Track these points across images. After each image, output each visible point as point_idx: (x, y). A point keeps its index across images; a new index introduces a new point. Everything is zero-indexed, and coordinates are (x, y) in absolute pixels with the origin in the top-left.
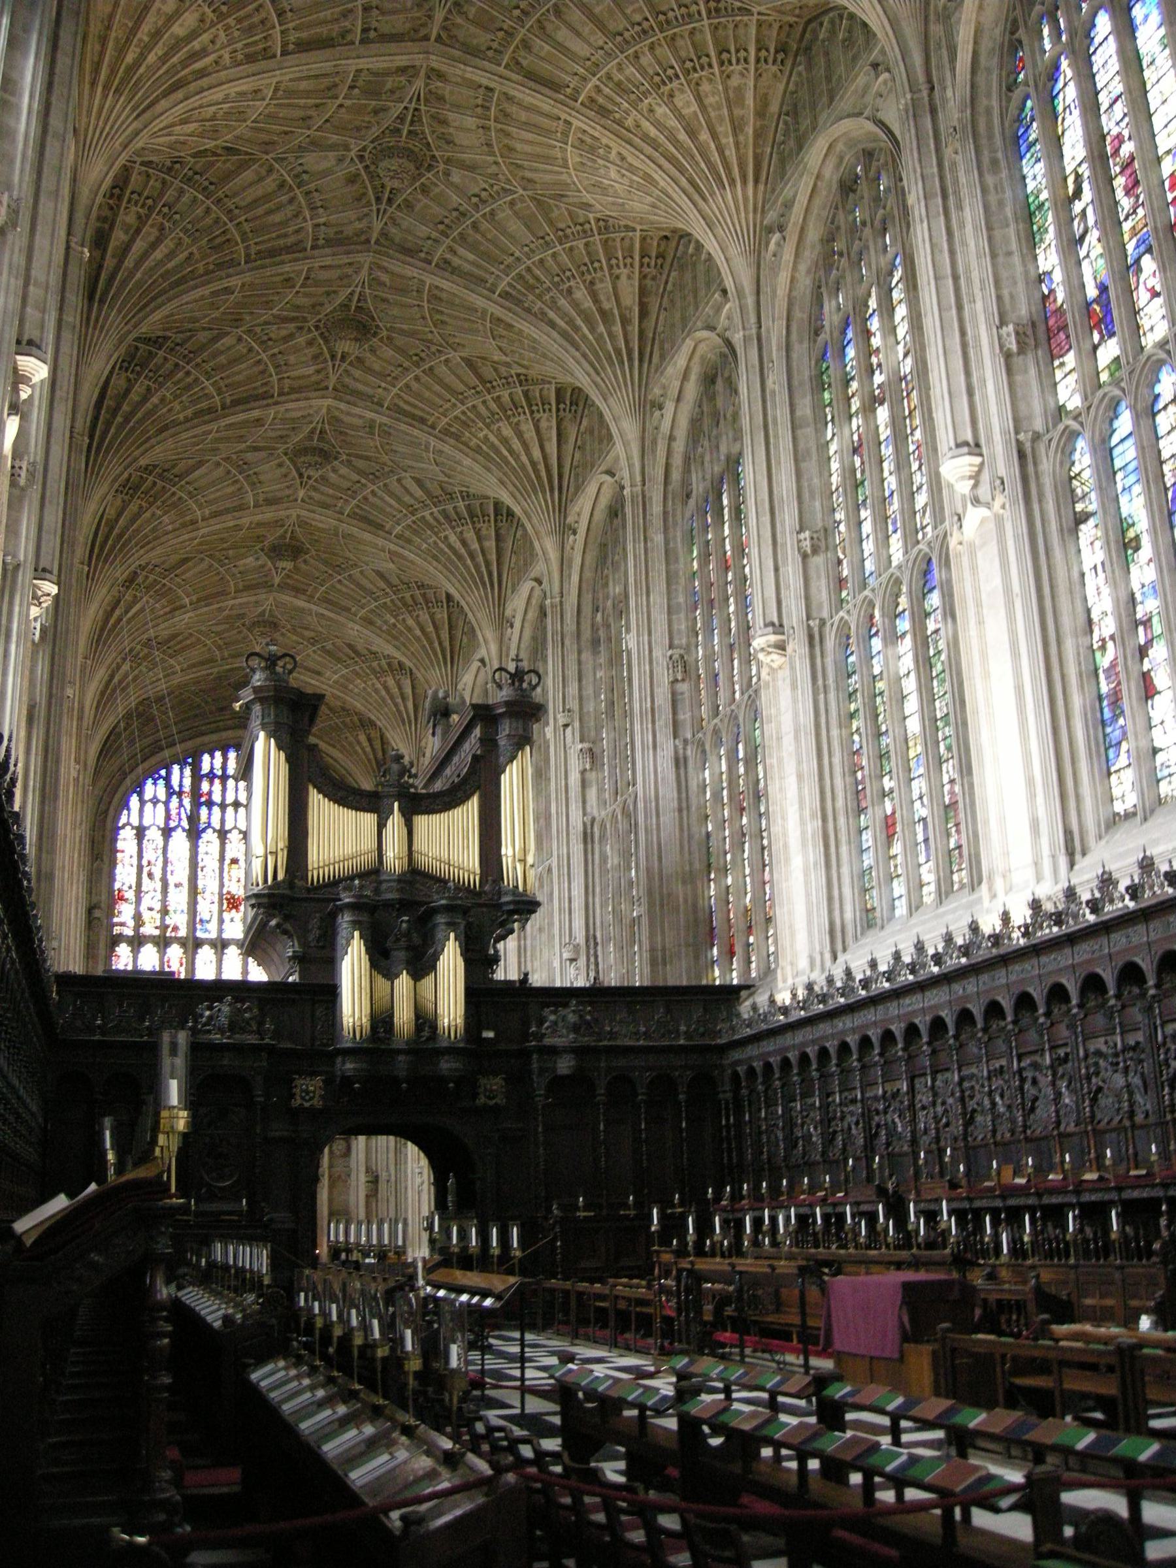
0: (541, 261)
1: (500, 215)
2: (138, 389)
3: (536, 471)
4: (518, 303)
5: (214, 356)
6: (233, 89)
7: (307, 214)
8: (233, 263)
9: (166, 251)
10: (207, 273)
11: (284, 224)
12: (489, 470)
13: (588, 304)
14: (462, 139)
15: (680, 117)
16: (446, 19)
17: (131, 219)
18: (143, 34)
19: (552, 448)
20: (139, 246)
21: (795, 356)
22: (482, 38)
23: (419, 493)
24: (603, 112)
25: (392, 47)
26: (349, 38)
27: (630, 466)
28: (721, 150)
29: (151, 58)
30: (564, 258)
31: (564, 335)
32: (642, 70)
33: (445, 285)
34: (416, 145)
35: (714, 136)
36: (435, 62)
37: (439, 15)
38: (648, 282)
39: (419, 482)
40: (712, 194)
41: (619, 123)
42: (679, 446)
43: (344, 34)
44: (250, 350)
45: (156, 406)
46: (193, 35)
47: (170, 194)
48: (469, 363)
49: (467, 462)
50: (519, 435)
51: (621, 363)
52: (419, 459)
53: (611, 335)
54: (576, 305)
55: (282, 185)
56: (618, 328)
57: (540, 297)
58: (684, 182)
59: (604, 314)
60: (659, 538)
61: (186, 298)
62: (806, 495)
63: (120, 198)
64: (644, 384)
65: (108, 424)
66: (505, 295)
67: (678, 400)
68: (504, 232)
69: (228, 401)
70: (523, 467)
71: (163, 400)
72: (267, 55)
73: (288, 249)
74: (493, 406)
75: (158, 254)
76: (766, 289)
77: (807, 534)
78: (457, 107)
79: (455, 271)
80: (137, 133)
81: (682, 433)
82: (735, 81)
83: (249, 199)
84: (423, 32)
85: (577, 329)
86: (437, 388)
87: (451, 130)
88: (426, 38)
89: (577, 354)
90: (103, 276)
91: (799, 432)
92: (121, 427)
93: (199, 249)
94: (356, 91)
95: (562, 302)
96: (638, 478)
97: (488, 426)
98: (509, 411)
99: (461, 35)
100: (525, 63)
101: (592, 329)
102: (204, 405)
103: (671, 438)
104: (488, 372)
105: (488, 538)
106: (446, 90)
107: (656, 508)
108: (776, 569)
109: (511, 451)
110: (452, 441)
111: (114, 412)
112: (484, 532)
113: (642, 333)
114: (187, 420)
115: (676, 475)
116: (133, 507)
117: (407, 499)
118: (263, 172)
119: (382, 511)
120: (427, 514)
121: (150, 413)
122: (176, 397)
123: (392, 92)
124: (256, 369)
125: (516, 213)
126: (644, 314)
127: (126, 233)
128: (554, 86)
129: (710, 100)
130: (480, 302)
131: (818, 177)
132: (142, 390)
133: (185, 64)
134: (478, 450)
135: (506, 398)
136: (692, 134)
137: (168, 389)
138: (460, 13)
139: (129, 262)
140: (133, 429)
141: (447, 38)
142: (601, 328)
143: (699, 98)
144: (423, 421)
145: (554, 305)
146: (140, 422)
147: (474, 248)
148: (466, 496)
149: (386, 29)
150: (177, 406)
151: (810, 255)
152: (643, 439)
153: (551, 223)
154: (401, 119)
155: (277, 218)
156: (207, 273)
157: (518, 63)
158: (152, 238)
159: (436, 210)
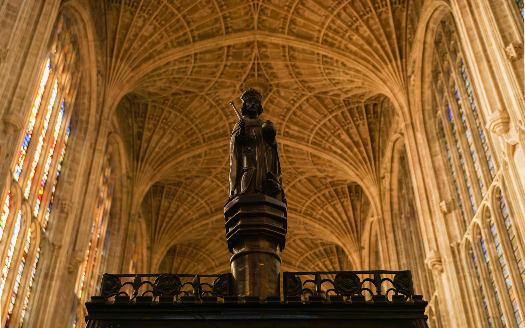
0: (325, 124)
1: (304, 107)
2: (173, 206)
3: (346, 225)
4: (320, 146)
5: (203, 188)
7: (225, 118)
8: (198, 143)
9: (167, 139)
10: (188, 148)
11: (216, 123)
12: (326, 228)
13: (348, 140)
14: (280, 75)
16: (259, 18)
17: (151, 126)
19: (351, 214)
20: (156, 137)
21: (428, 126)
23: (303, 246)
24: (332, 45)
25: (240, 34)
26: (221, 32)
27: (376, 207)
28: (383, 48)
29: (135, 45)
30: (334, 121)
31: (341, 156)
32: (343, 21)
33: (288, 143)
34: (262, 80)
35: (379, 42)
37: (256, 17)
38: (372, 126)
39: (302, 241)
40: (383, 68)
41: (339, 48)
42: (395, 193)
43: (219, 30)
44: (218, 186)
45: (182, 214)
47: (165, 114)
48: (309, 180)
49: (317, 226)
50: (336, 210)
51: (366, 163)
52: (299, 229)
53: (360, 152)
54: (343, 141)
55: (212, 106)
56: (362, 148)
57: (327, 141)
58: (370, 66)
59: (356, 144)
60: (391, 236)
61: (180, 159)
62: (442, 186)
63: (145, 117)
64: (377, 170)
65: (163, 221)
66: (314, 143)
67: (391, 172)
68: (307, 114)
69: (213, 209)
70: (339, 224)
71: (185, 210)
72: (186, 41)
73: (221, 136)
74: (323, 198)
75: (165, 140)
76: (412, 102)
77: (443, 203)
78: (274, 59)
79: (292, 136)
80: (132, 77)
81: (395, 186)
82: (384, 16)
83: (199, 114)
84: (251, 26)
85: (345, 152)
86: (299, 194)
87: (275, 71)
88: (253, 28)
89: (348, 164)
90: (142, 150)
91: (435, 159)
92: (168, 223)
93: (182, 136)
94: (230, 58)
95: (337, 141)
96: (380, 212)
97: (322, 208)
98: (329, 199)
99: (267, 24)
100: (295, 31)
101: (352, 151)
102: (202, 211)
103: (391, 190)
104: (318, 184)
105: (335, 263)
107: (388, 222)
108: (433, 224)
109: (334, 218)
110: (309, 218)
111: (164, 216)
112: (333, 260)
113: (373, 149)
114: (197, 219)
115: (396, 206)
116: (185, 262)
117: (299, 249)
118: (202, 101)
119: (290, 256)
120: (308, 254)
121: (180, 216)
122: (190, 208)
123: (246, 56)
124: (222, 194)
125: (310, 105)
126: (373, 140)
127: (150, 132)
129: (375, 27)
130: (305, 148)
131: (425, 43)
132: (175, 206)
134: (320, 220)
135: (327, 194)
136: (370, 44)
137: (186, 205)
138: (265, 14)
139: (153, 144)
140: (173, 224)
141: (262, 26)
142: (356, 150)
144: (295, 210)
145: (334, 143)
146: (176, 220)
147: (296, 124)
148: (323, 244)
149: (236, 27)
150: (190, 211)
151: (428, 79)
152: (380, 195)
153: (326, 106)
154: (253, 69)
155: (213, 121)
156: (188, 148)
157: (292, 32)
158: (161, 134)
159: (278, 110)
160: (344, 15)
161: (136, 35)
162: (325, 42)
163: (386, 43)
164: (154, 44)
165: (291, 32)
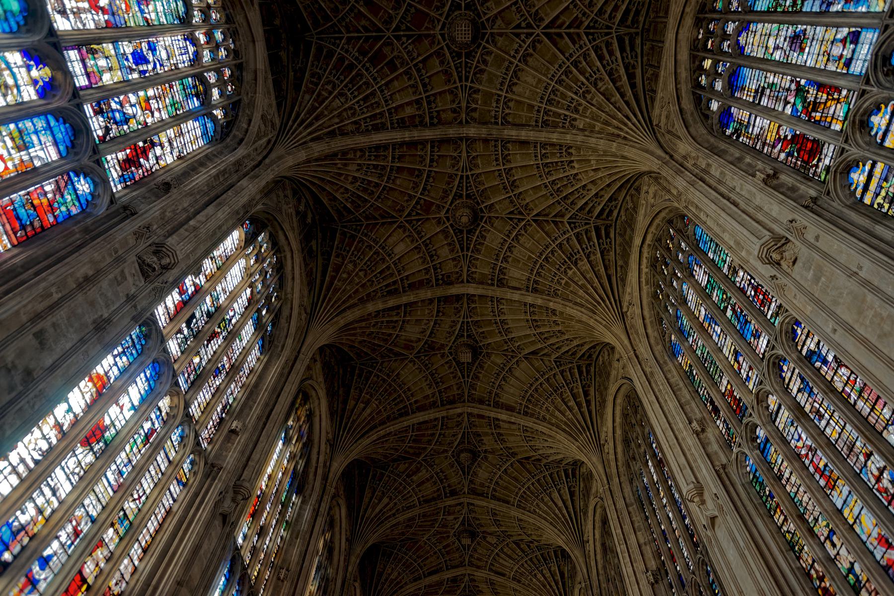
6: (412, 590)
15: (540, 581)
18: (382, 580)
22: (480, 564)
24: (519, 582)
25: (456, 570)
36: (468, 572)
46: (397, 578)
72: (420, 578)
82: (552, 569)
106: (476, 578)
128: (503, 575)
133: (395, 586)
136: (544, 586)
141: (471, 564)
143: (543, 576)
160: (526, 565)
161: (386, 580)
162: (514, 579)
163: (555, 587)
164: (398, 583)
165: (490, 570)
